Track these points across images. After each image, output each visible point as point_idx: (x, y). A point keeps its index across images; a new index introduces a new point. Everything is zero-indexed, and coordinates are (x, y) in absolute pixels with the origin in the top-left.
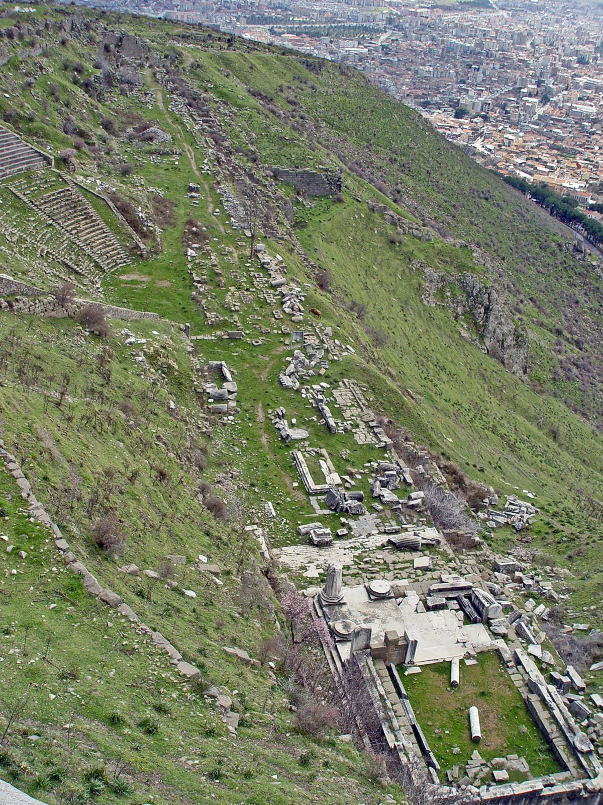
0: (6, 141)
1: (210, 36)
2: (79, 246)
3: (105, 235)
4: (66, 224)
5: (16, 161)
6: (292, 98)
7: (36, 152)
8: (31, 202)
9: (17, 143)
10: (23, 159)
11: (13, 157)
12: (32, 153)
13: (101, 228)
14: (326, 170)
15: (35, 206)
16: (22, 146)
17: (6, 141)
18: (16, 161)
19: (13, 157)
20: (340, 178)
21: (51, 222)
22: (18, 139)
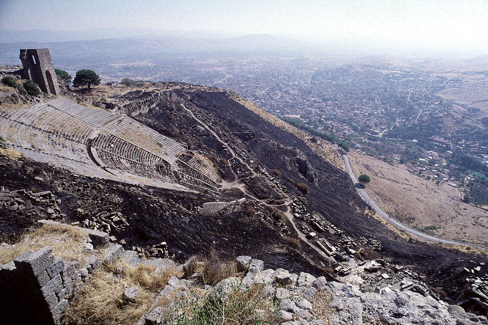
7: (181, 145)
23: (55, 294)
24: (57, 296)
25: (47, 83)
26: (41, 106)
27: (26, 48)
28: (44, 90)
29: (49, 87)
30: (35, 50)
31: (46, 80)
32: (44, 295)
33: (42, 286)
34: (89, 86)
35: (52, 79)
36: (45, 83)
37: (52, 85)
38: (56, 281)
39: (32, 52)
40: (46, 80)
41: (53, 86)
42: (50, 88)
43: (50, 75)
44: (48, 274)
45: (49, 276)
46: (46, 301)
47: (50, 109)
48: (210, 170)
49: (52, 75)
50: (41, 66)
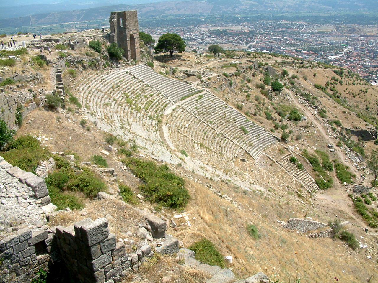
0: (261, 132)
1: (293, 62)
2: (299, 182)
3: (308, 176)
4: (292, 172)
5: (266, 141)
6: (332, 88)
7: (273, 136)
8: (277, 161)
9: (265, 132)
10: (269, 140)
11: (265, 140)
12: (271, 137)
13: (306, 173)
14: (370, 129)
15: (279, 163)
16: (267, 134)
17: (261, 132)
18: (266, 141)
19: (265, 140)
20: (377, 132)
21: (286, 171)
22: (264, 130)
23: (104, 271)
24: (106, 275)
25: (129, 48)
26: (119, 72)
27: (116, 11)
28: (126, 56)
29: (130, 52)
30: (125, 12)
31: (129, 44)
32: (95, 269)
33: (94, 258)
34: (171, 53)
35: (134, 44)
36: (127, 48)
37: (134, 50)
38: (105, 258)
39: (122, 15)
40: (129, 44)
41: (135, 51)
42: (131, 54)
43: (134, 39)
44: (100, 248)
45: (101, 250)
46: (94, 275)
47: (129, 77)
48: (306, 174)
49: (135, 39)
50: (127, 29)
